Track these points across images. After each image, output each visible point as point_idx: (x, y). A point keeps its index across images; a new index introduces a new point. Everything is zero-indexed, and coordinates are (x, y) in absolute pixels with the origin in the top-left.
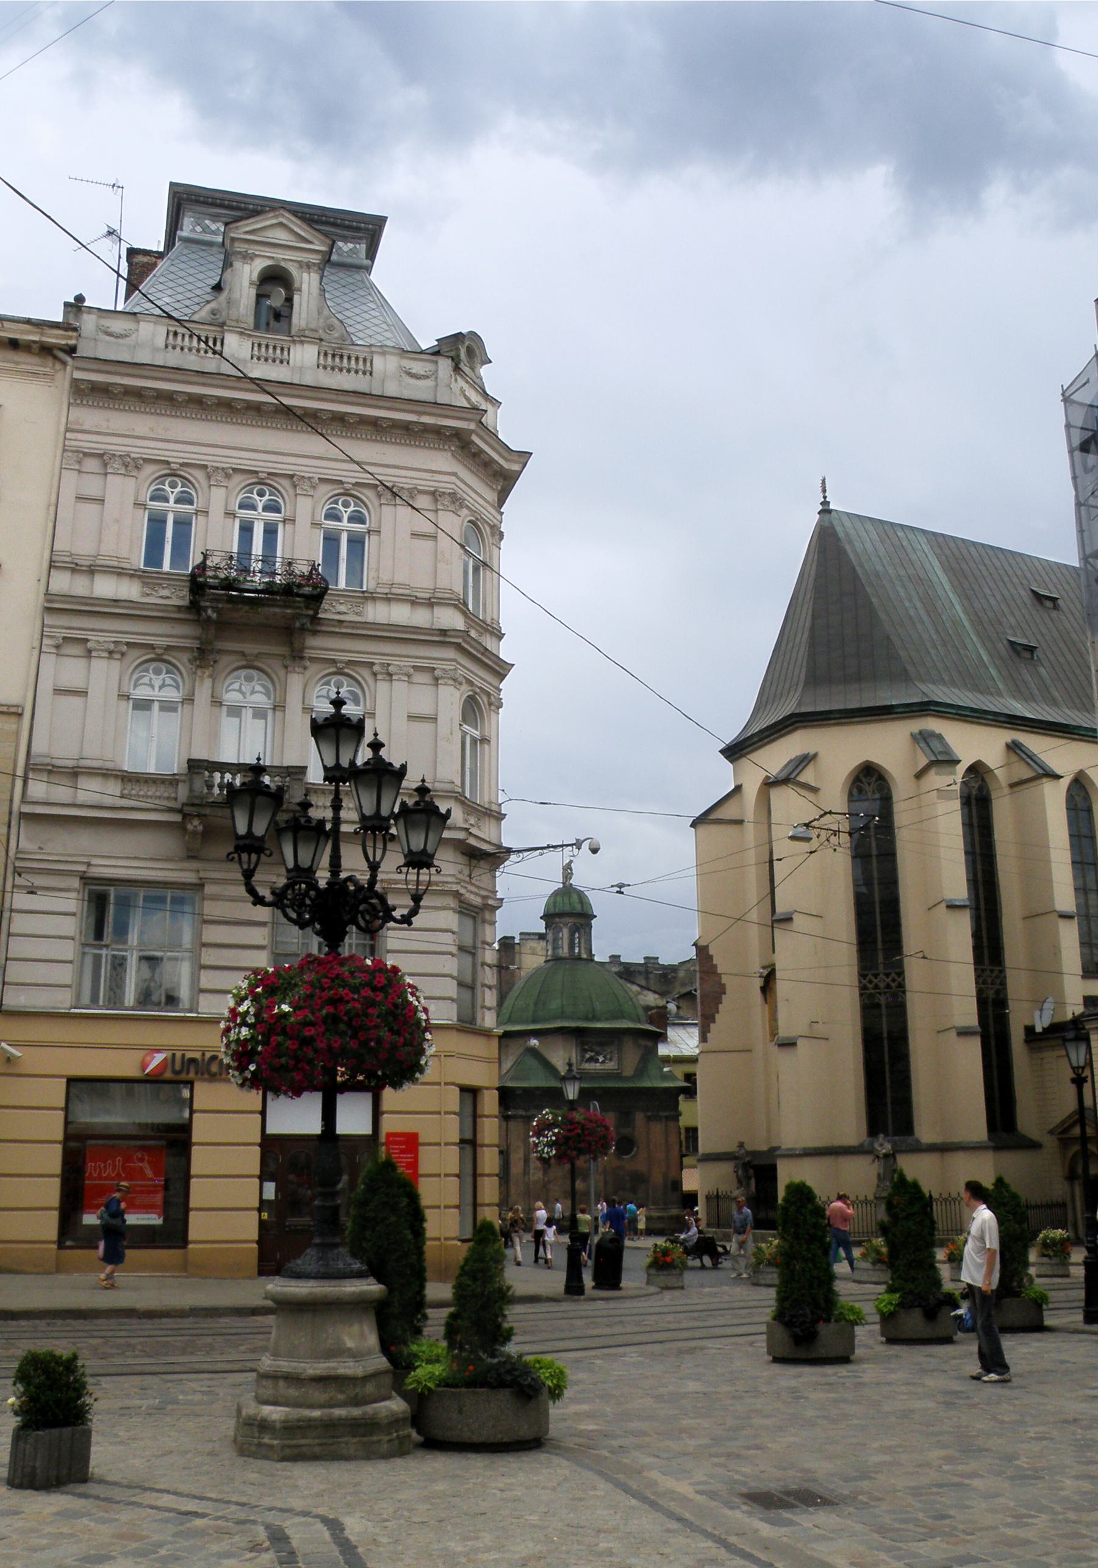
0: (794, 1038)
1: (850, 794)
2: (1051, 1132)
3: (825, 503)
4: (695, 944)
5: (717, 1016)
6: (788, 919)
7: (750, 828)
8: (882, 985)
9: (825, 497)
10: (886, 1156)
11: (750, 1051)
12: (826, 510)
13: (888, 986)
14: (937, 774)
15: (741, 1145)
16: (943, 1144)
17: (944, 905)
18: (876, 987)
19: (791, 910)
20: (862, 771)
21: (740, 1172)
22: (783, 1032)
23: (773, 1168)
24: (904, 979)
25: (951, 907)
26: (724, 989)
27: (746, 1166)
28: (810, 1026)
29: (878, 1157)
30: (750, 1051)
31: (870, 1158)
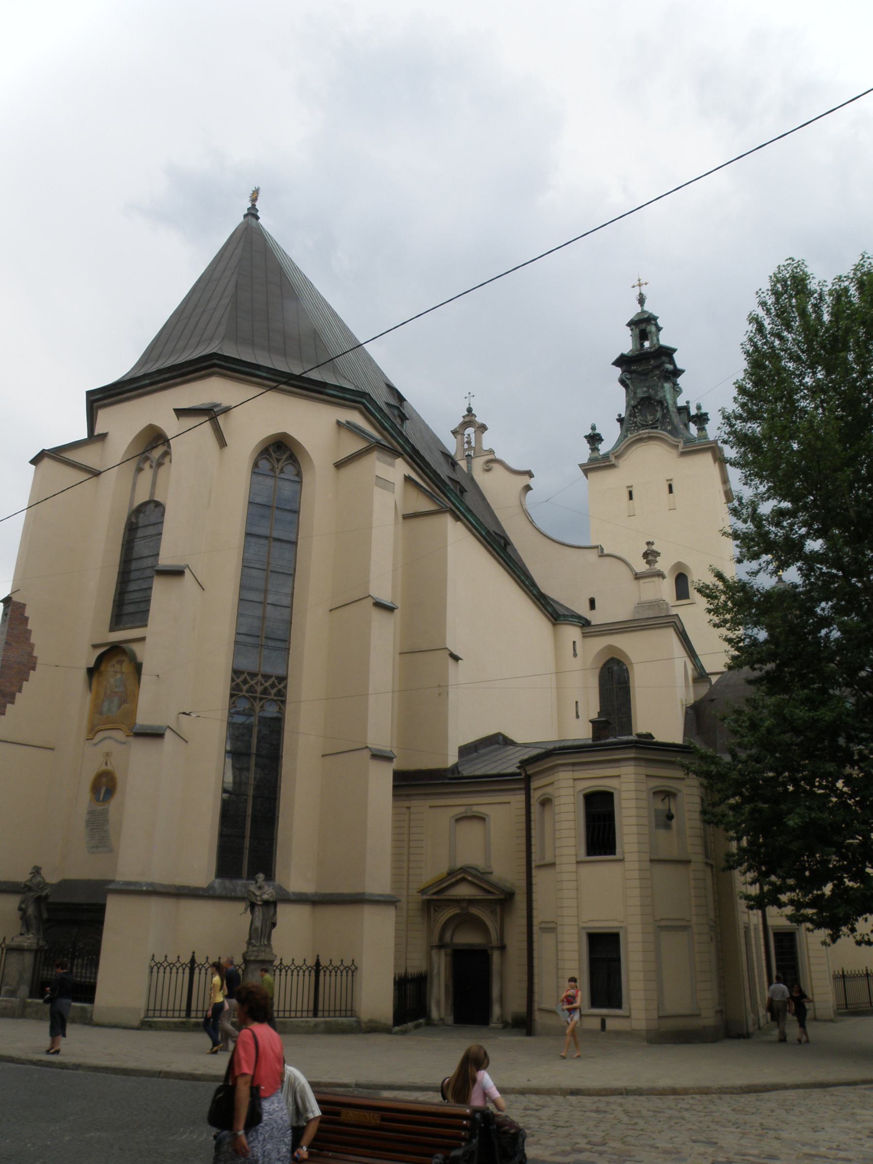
0: (160, 727)
1: (256, 465)
2: (423, 891)
3: (252, 213)
4: (7, 601)
5: (18, 694)
6: (177, 573)
7: (109, 479)
8: (259, 689)
9: (254, 206)
10: (266, 903)
11: (53, 749)
12: (252, 213)
13: (265, 691)
14: (379, 459)
15: (37, 871)
16: (316, 894)
17: (370, 602)
18: (251, 690)
19: (182, 564)
20: (273, 444)
21: (31, 911)
22: (144, 718)
23: (101, 909)
24: (285, 687)
25: (378, 605)
26: (35, 663)
27: (39, 901)
28: (178, 718)
29: (253, 906)
30: (53, 749)
31: (241, 906)
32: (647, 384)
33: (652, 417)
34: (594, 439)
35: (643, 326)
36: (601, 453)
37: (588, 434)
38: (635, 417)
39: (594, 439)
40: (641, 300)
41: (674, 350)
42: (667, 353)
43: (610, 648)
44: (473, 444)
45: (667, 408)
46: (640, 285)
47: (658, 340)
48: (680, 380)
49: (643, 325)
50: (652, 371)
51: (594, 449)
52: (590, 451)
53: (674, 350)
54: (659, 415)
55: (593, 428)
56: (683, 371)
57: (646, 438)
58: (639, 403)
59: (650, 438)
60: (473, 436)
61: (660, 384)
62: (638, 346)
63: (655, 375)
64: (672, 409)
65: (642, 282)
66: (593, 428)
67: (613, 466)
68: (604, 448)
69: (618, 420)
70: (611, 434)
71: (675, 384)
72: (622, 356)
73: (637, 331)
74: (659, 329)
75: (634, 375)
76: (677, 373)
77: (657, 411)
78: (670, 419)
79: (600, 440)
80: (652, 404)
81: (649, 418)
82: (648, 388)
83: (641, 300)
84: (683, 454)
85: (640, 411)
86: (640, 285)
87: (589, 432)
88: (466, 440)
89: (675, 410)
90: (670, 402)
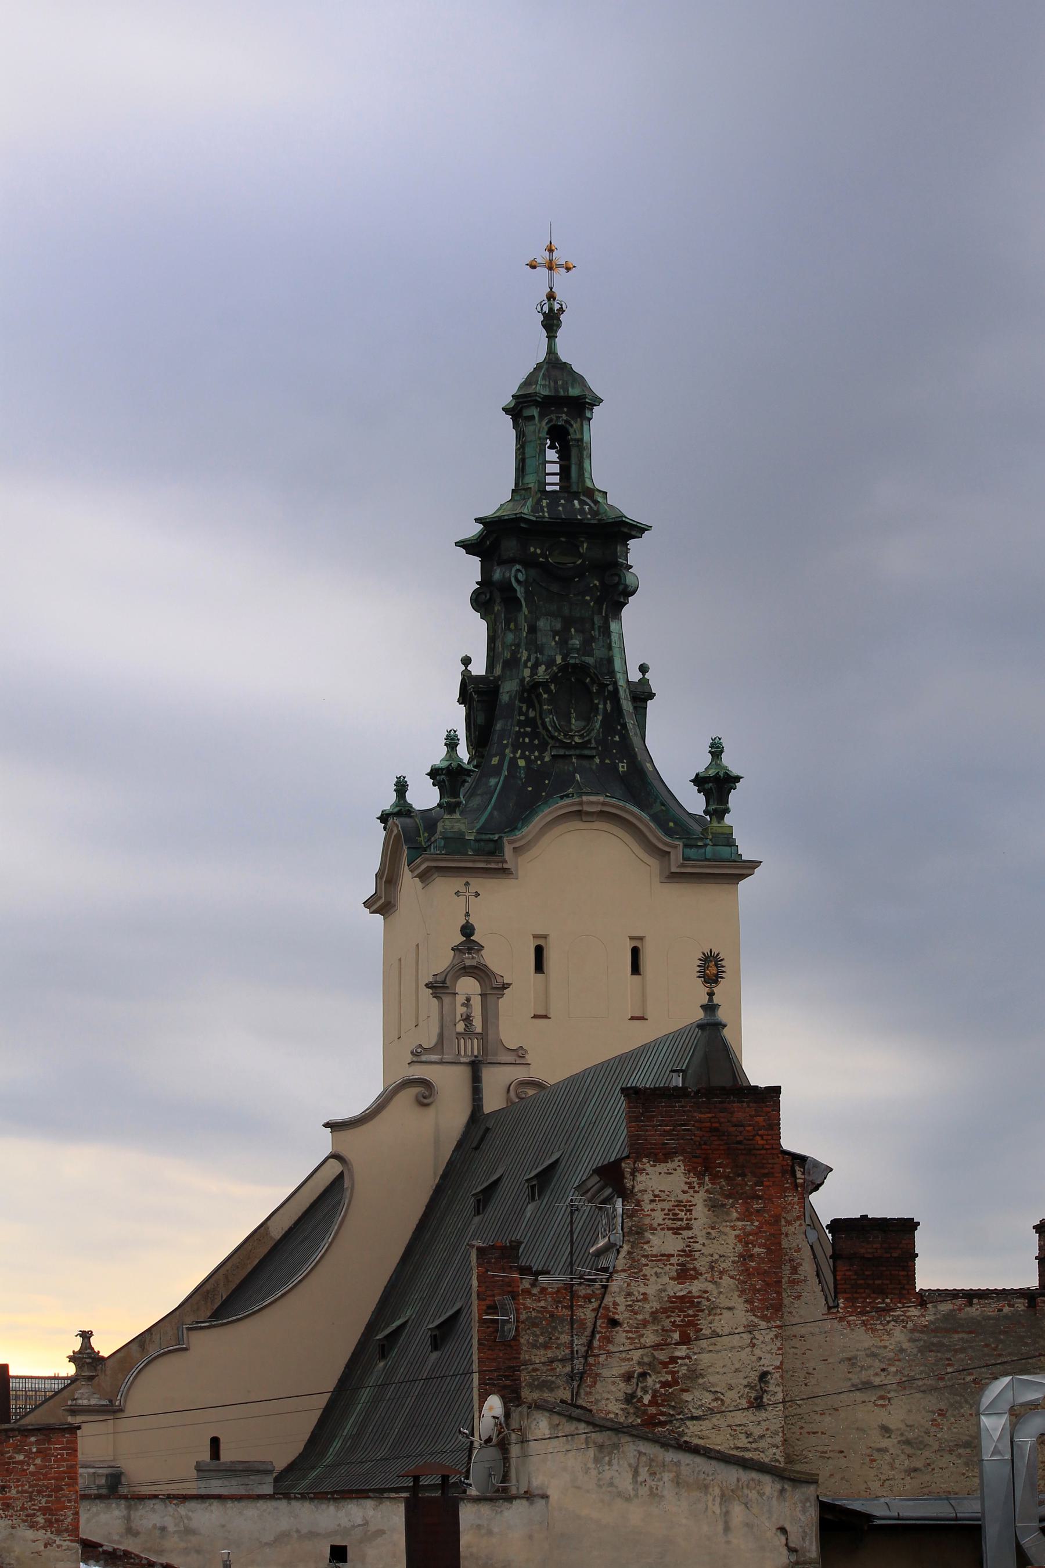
32: (566, 611)
40: (551, 322)
44: (478, 1025)
49: (553, 409)
59: (604, 815)
60: (476, 1002)
83: (551, 322)
84: (674, 877)
88: (461, 1010)
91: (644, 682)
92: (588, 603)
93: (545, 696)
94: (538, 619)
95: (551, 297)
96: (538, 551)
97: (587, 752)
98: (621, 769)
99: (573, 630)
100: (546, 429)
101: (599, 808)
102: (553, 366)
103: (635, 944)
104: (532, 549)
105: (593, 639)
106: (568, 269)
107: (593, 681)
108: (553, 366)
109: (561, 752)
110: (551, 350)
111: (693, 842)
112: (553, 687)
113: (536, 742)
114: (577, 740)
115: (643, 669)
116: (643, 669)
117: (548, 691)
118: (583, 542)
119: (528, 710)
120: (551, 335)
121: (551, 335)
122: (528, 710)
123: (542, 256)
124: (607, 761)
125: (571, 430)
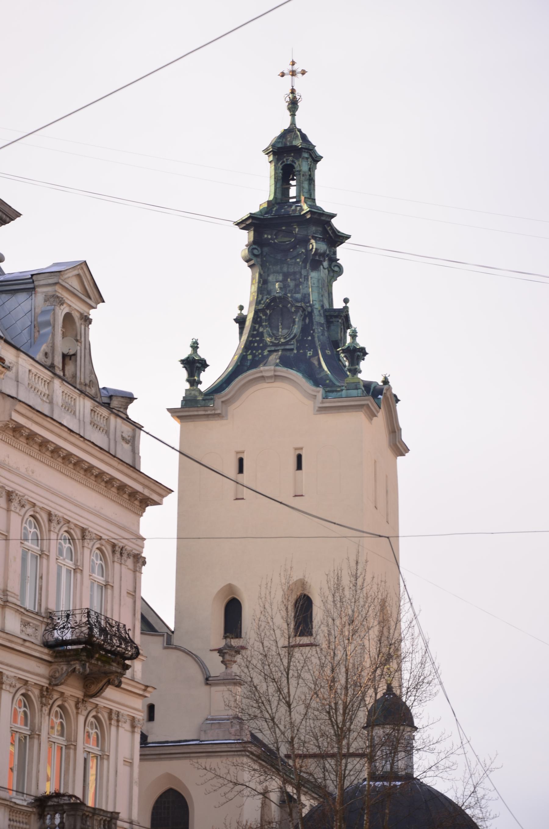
32: (285, 269)
33: (285, 331)
34: (194, 365)
35: (289, 160)
36: (203, 387)
37: (184, 357)
38: (261, 325)
39: (194, 365)
40: (293, 105)
41: (333, 216)
42: (322, 221)
43: (169, 777)
45: (310, 315)
46: (293, 73)
47: (311, 180)
48: (342, 252)
49: (292, 156)
50: (294, 248)
51: (193, 381)
52: (187, 386)
53: (333, 216)
54: (296, 329)
55: (195, 346)
56: (348, 237)
57: (270, 377)
58: (268, 306)
59: (276, 377)
61: (304, 272)
62: (279, 196)
63: (298, 255)
64: (318, 318)
65: (298, 68)
66: (195, 346)
67: (218, 416)
68: (208, 379)
69: (236, 320)
70: (222, 354)
71: (333, 260)
72: (252, 216)
73: (280, 166)
74: (316, 159)
75: (266, 249)
76: (339, 238)
77: (294, 322)
78: (313, 337)
79: (203, 365)
80: (289, 311)
81: (282, 332)
82: (286, 276)
83: (293, 105)
85: (269, 319)
86: (293, 73)
87: (187, 352)
89: (322, 320)
90: (317, 306)
91: (346, 309)
92: (298, 263)
93: (264, 317)
94: (268, 275)
95: (293, 91)
96: (269, 237)
97: (288, 347)
98: (308, 355)
99: (289, 280)
100: (281, 167)
101: (271, 374)
102: (292, 131)
103: (298, 452)
104: (266, 236)
105: (301, 283)
106: (303, 74)
107: (292, 306)
108: (292, 131)
109: (273, 348)
110: (293, 123)
111: (334, 389)
112: (268, 312)
113: (261, 345)
114: (283, 340)
115: (346, 301)
116: (346, 301)
117: (265, 314)
118: (295, 228)
119: (259, 328)
120: (293, 115)
121: (293, 115)
122: (259, 328)
123: (287, 68)
124: (301, 351)
125: (295, 166)
